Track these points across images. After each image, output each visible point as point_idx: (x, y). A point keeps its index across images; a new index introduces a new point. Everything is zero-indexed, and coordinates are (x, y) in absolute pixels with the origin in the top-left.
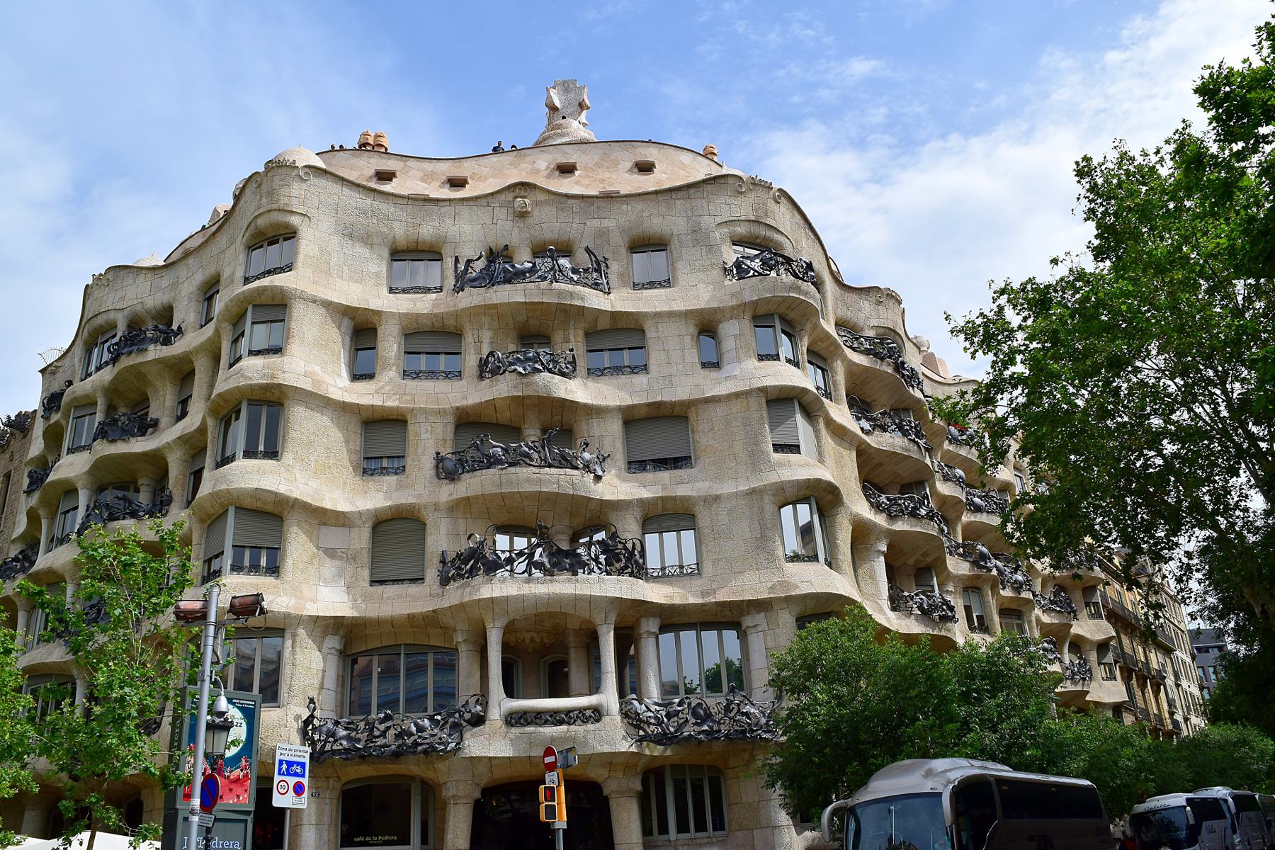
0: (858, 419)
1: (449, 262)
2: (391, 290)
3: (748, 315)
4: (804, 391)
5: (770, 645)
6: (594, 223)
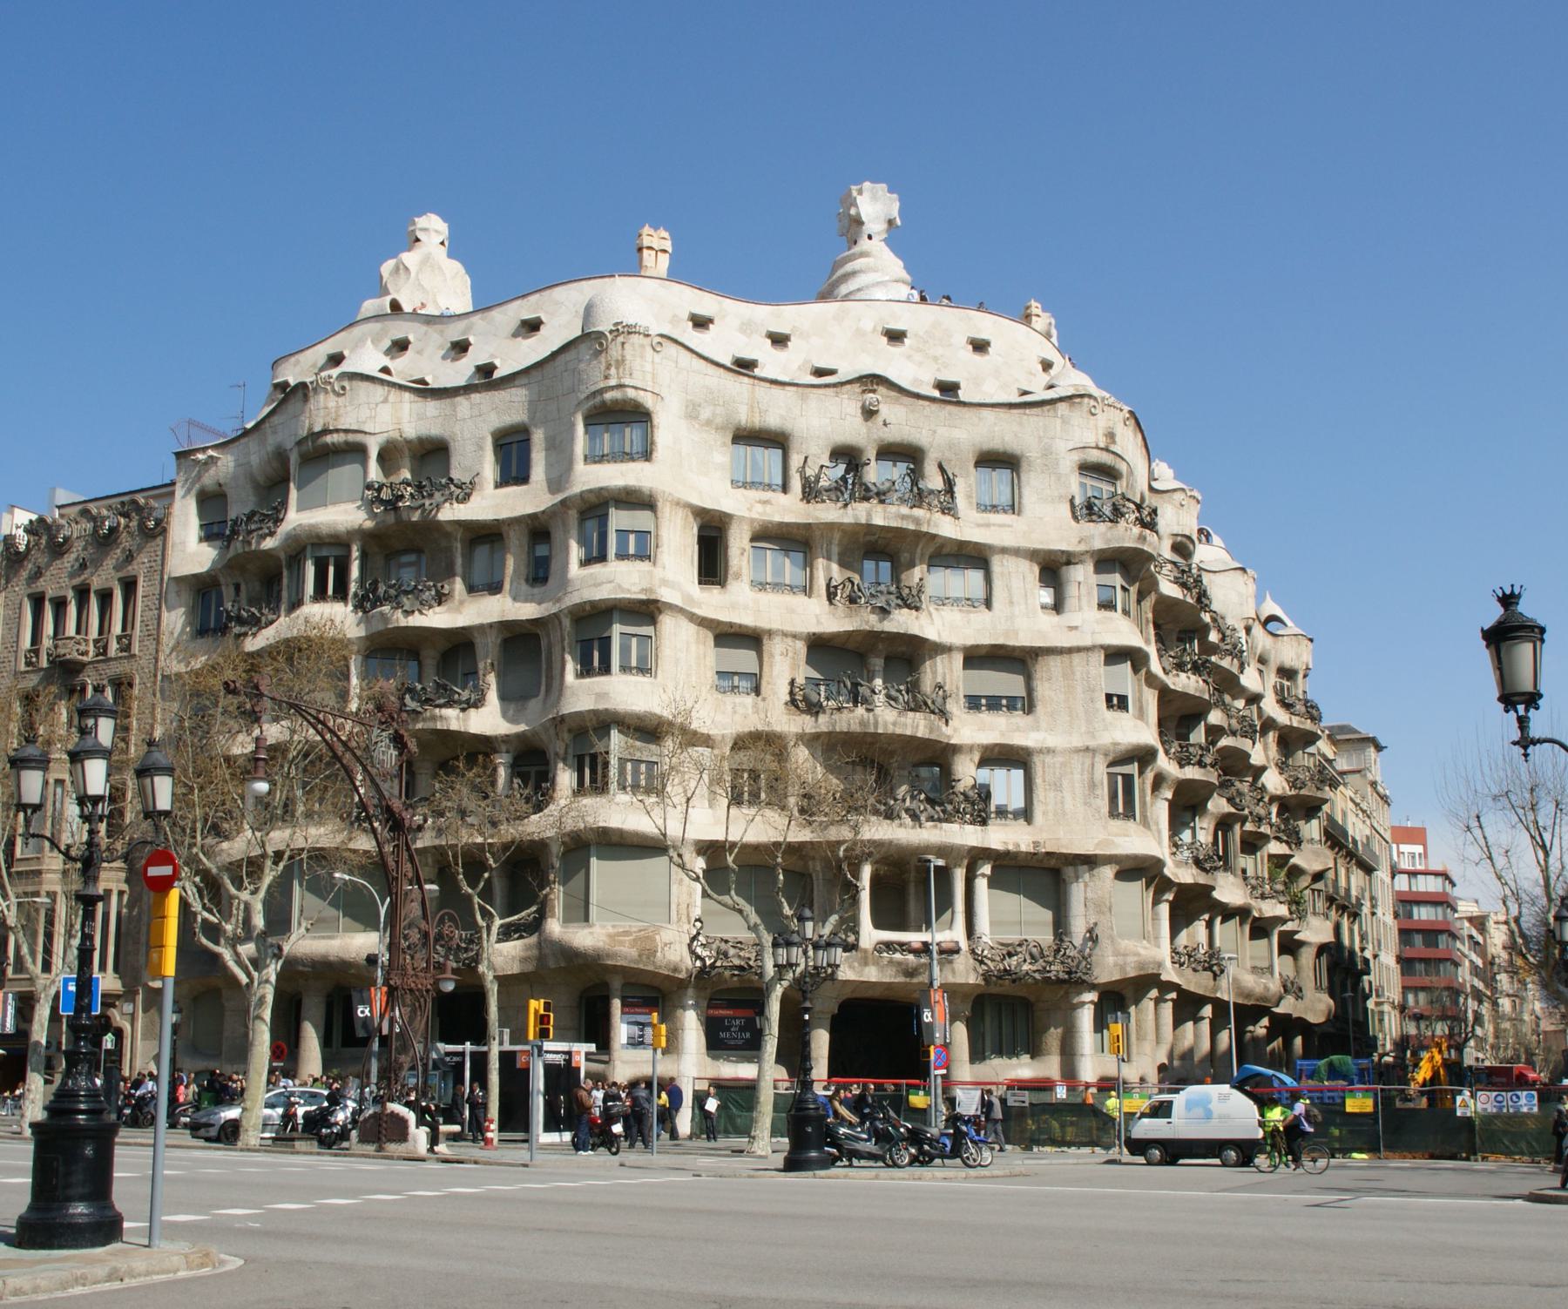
0: (1160, 656)
4: (1139, 650)
5: (1089, 895)
6: (942, 431)
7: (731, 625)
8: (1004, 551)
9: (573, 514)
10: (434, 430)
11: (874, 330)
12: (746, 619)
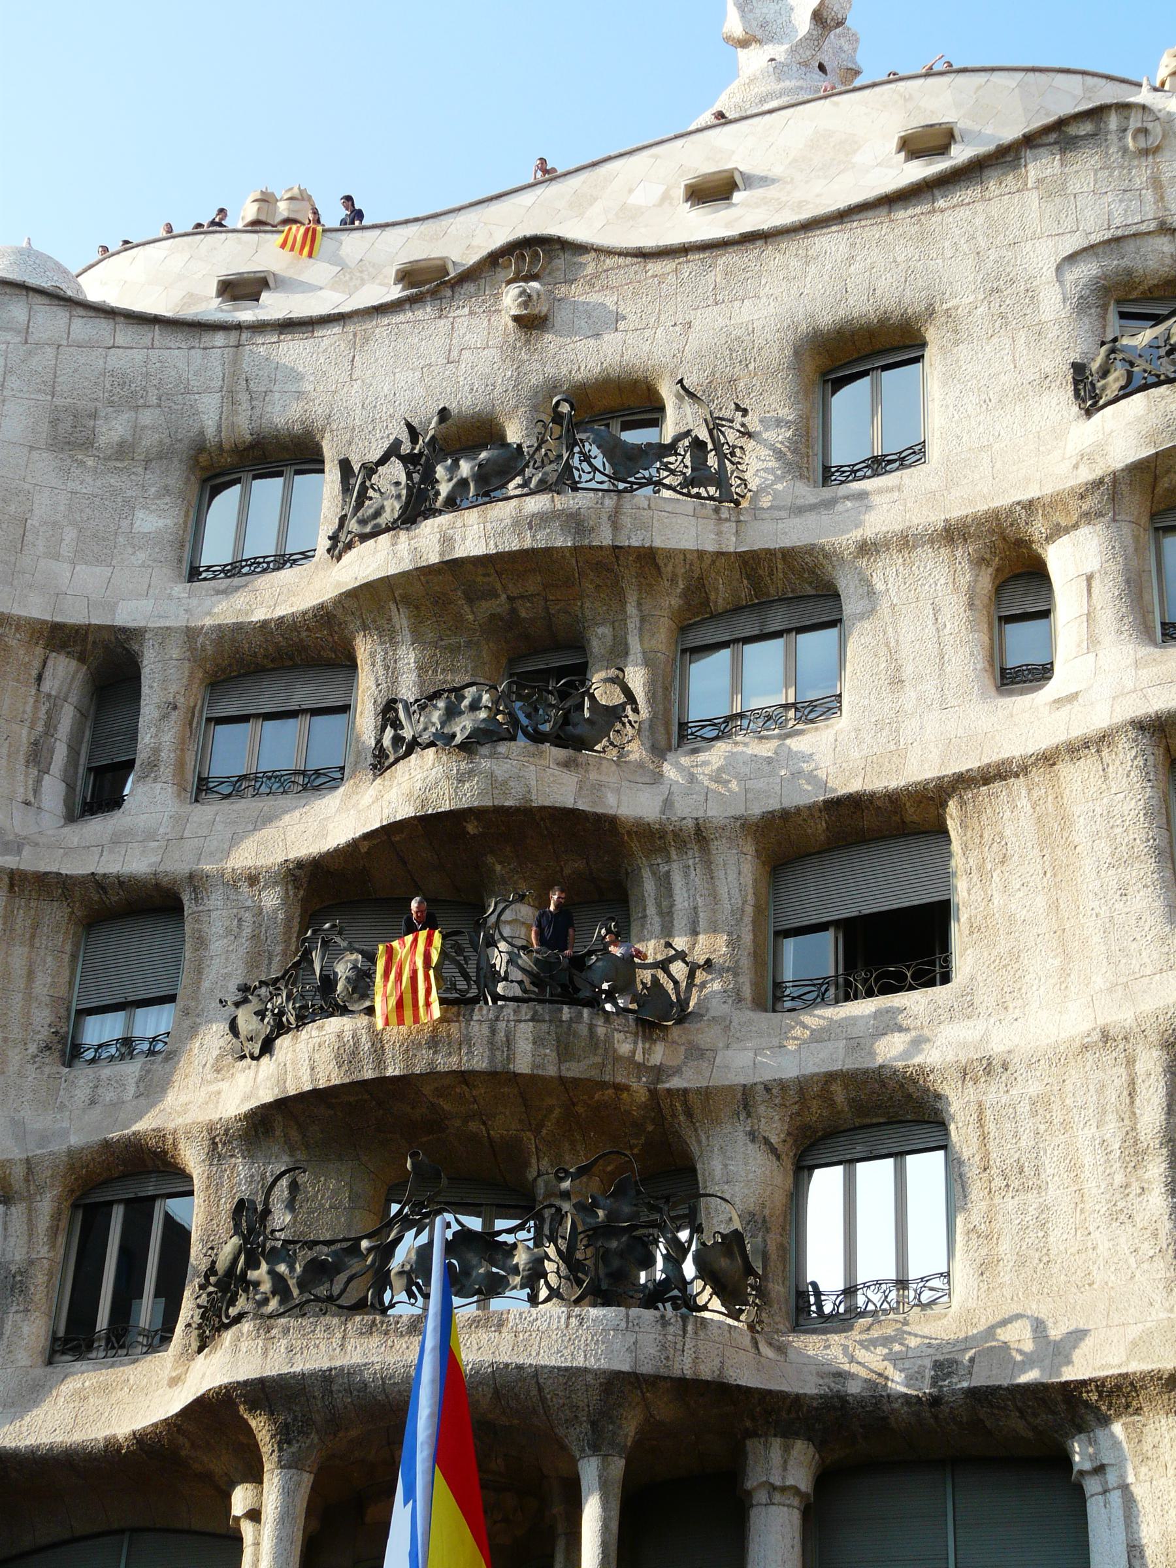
2: (194, 574)
3: (1135, 504)
7: (98, 882)
8: (866, 549)
11: (666, 197)
12: (136, 863)
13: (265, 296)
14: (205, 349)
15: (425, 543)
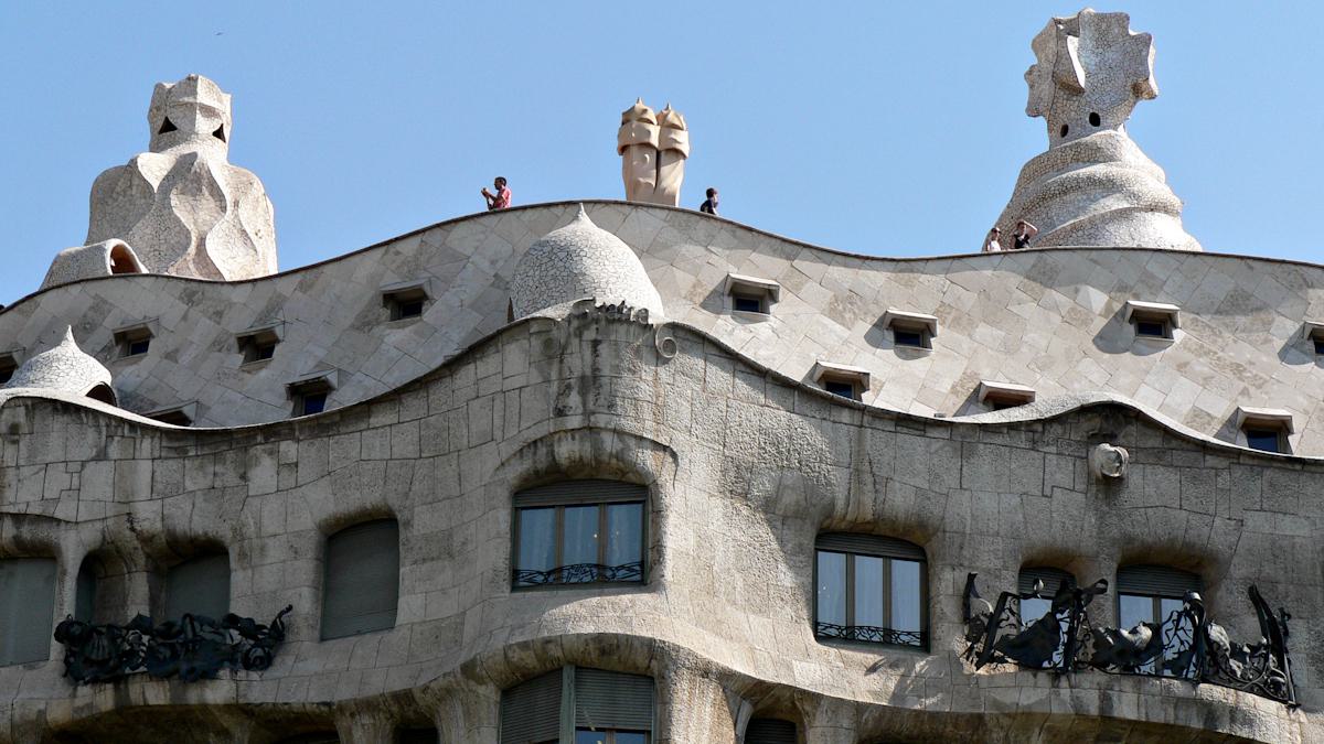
1: (948, 583)
6: (1257, 523)
9: (489, 693)
10: (194, 518)
13: (773, 308)
14: (834, 422)
15: (1087, 691)
